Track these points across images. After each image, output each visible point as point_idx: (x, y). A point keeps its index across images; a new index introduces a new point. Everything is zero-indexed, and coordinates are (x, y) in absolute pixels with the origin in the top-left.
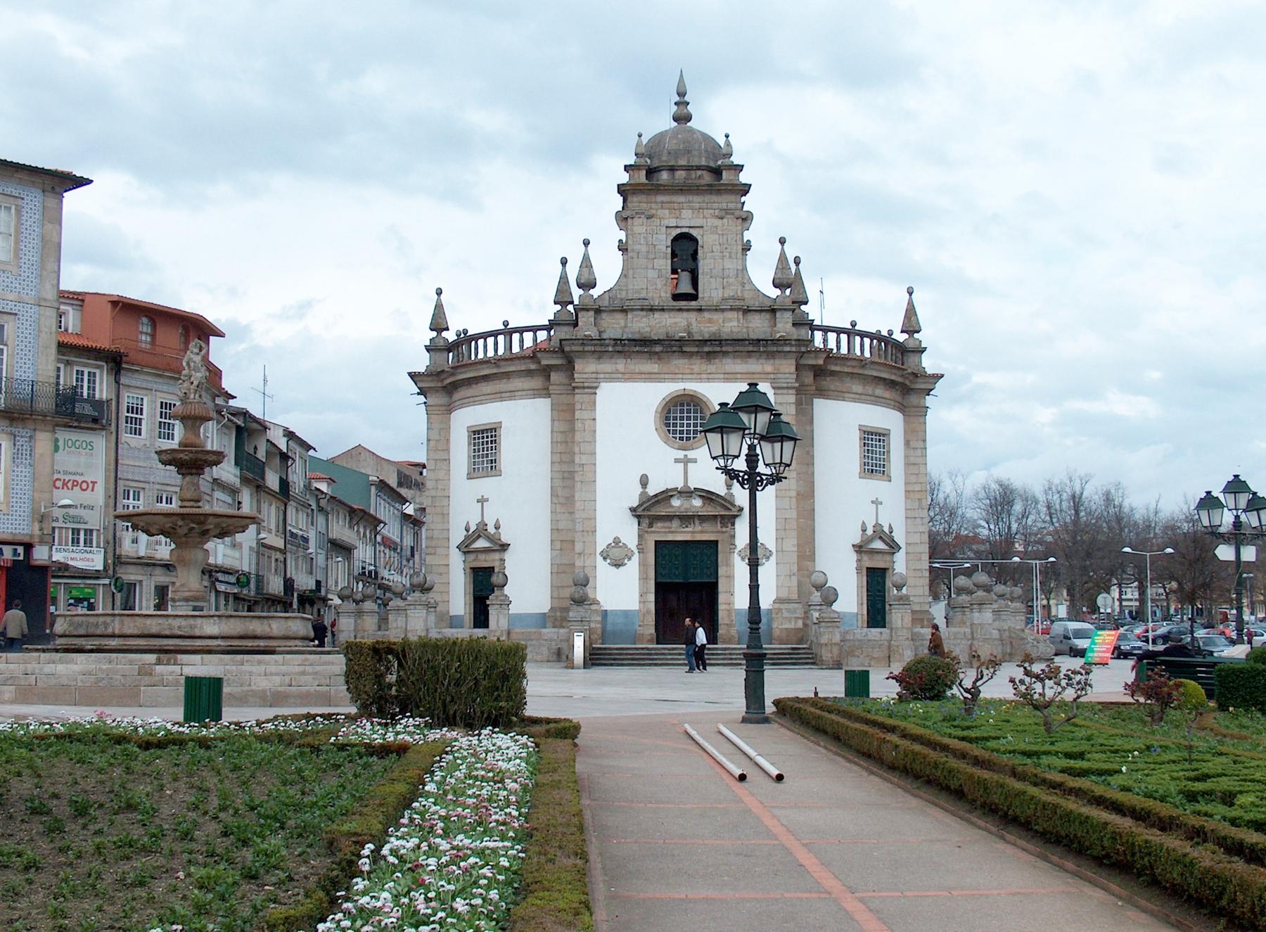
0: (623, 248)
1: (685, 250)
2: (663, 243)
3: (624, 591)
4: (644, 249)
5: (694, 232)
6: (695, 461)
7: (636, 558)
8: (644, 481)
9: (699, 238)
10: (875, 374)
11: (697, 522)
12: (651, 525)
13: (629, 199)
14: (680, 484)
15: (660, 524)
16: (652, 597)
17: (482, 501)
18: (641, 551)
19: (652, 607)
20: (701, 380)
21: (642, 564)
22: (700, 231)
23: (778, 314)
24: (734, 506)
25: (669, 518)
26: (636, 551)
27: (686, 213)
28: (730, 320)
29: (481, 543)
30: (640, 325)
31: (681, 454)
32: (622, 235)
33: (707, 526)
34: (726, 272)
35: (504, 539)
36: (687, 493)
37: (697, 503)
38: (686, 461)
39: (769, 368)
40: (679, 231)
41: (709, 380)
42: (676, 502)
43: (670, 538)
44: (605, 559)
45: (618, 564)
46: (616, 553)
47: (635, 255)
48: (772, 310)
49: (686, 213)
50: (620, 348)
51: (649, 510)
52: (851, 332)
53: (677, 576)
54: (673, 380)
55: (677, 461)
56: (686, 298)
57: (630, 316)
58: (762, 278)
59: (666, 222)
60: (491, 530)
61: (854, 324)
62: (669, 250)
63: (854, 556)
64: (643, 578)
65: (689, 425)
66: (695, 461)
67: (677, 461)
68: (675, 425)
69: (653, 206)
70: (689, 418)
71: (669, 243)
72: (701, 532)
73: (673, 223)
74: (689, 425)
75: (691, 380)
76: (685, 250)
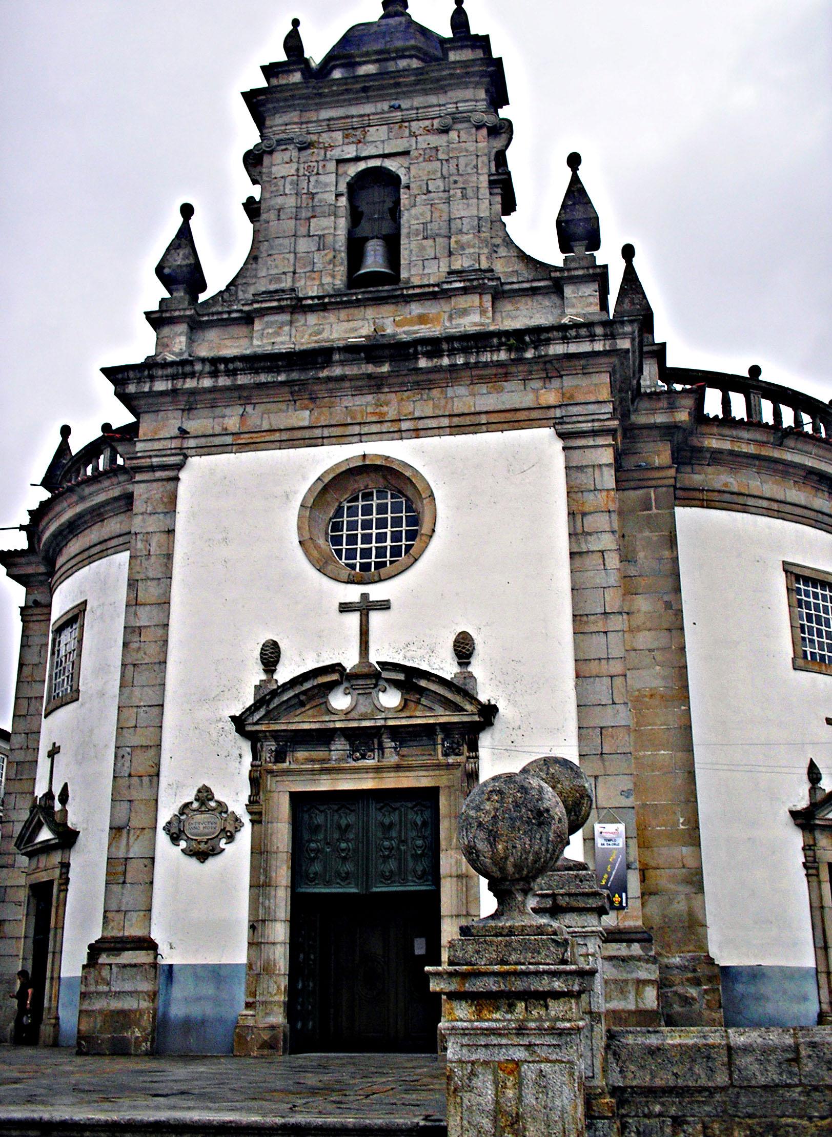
0: (252, 208)
1: (375, 195)
2: (331, 187)
3: (213, 918)
4: (291, 201)
5: (391, 165)
6: (385, 606)
7: (245, 836)
8: (271, 656)
9: (401, 173)
10: (809, 462)
11: (388, 743)
12: (280, 757)
13: (268, 123)
14: (351, 661)
15: (301, 755)
16: (280, 932)
17: (54, 752)
18: (257, 819)
19: (280, 956)
20: (400, 434)
21: (260, 851)
22: (400, 160)
23: (568, 291)
24: (473, 699)
25: (323, 737)
26: (246, 819)
27: (377, 134)
28: (464, 312)
29: (45, 835)
30: (276, 336)
31: (353, 593)
32: (256, 192)
33: (415, 754)
34: (456, 225)
35: (72, 821)
36: (368, 678)
37: (391, 699)
38: (365, 608)
39: (550, 397)
40: (362, 166)
41: (417, 433)
42: (340, 701)
43: (325, 785)
44: (175, 839)
45: (203, 853)
46: (201, 824)
47: (272, 215)
48: (552, 282)
49: (377, 134)
50: (223, 381)
51: (281, 719)
52: (751, 384)
53: (346, 878)
54: (341, 439)
55: (345, 608)
56: (372, 286)
57: (258, 325)
58: (534, 231)
59: (336, 153)
60: (58, 806)
61: (755, 370)
62: (343, 201)
63: (797, 839)
64: (260, 884)
65: (381, 538)
66: (385, 606)
67: (345, 608)
68: (352, 539)
69: (312, 127)
70: (382, 524)
71: (343, 188)
72: (398, 768)
73: (350, 152)
74: (381, 538)
75: (380, 435)
76: (375, 195)
